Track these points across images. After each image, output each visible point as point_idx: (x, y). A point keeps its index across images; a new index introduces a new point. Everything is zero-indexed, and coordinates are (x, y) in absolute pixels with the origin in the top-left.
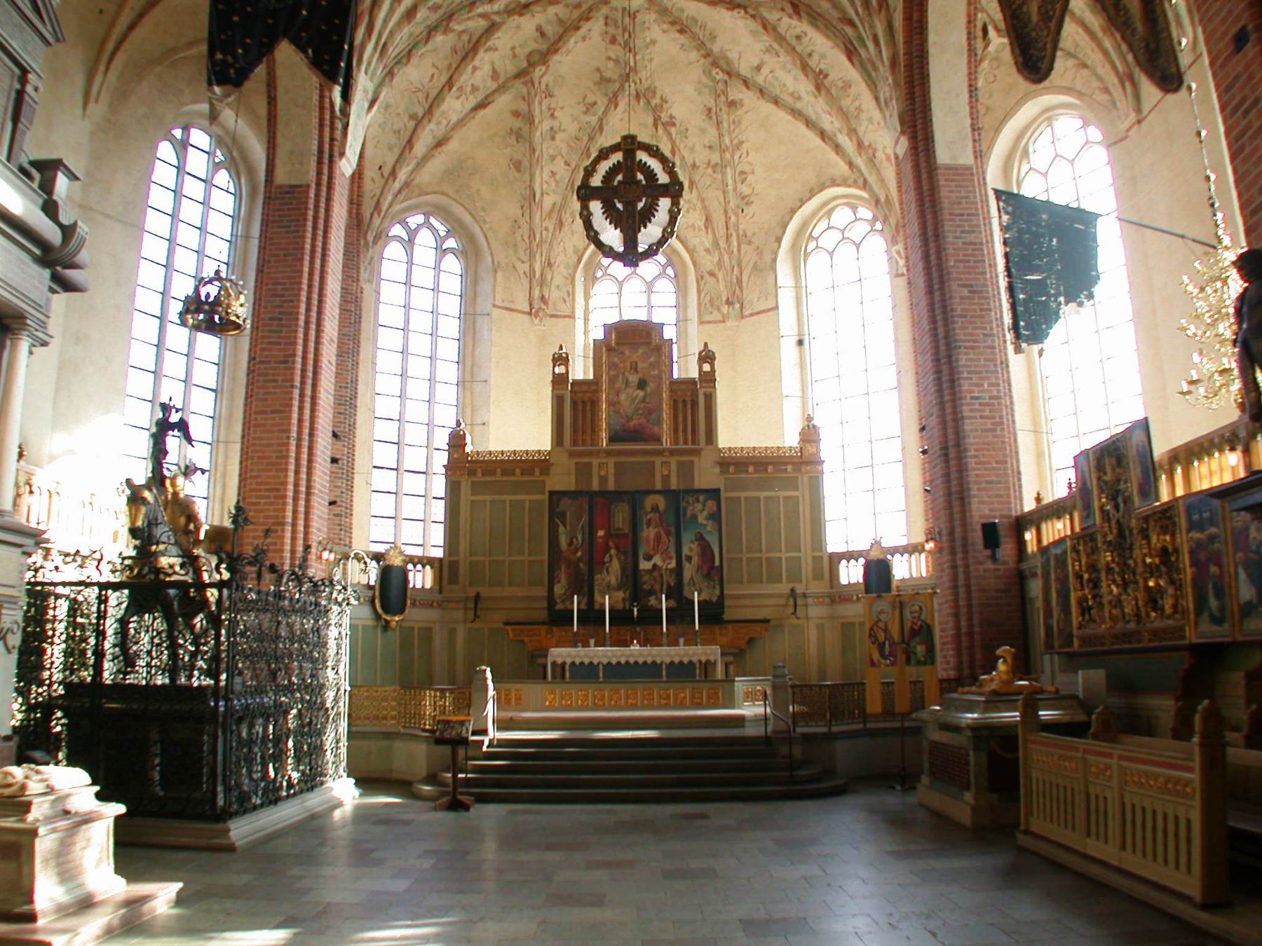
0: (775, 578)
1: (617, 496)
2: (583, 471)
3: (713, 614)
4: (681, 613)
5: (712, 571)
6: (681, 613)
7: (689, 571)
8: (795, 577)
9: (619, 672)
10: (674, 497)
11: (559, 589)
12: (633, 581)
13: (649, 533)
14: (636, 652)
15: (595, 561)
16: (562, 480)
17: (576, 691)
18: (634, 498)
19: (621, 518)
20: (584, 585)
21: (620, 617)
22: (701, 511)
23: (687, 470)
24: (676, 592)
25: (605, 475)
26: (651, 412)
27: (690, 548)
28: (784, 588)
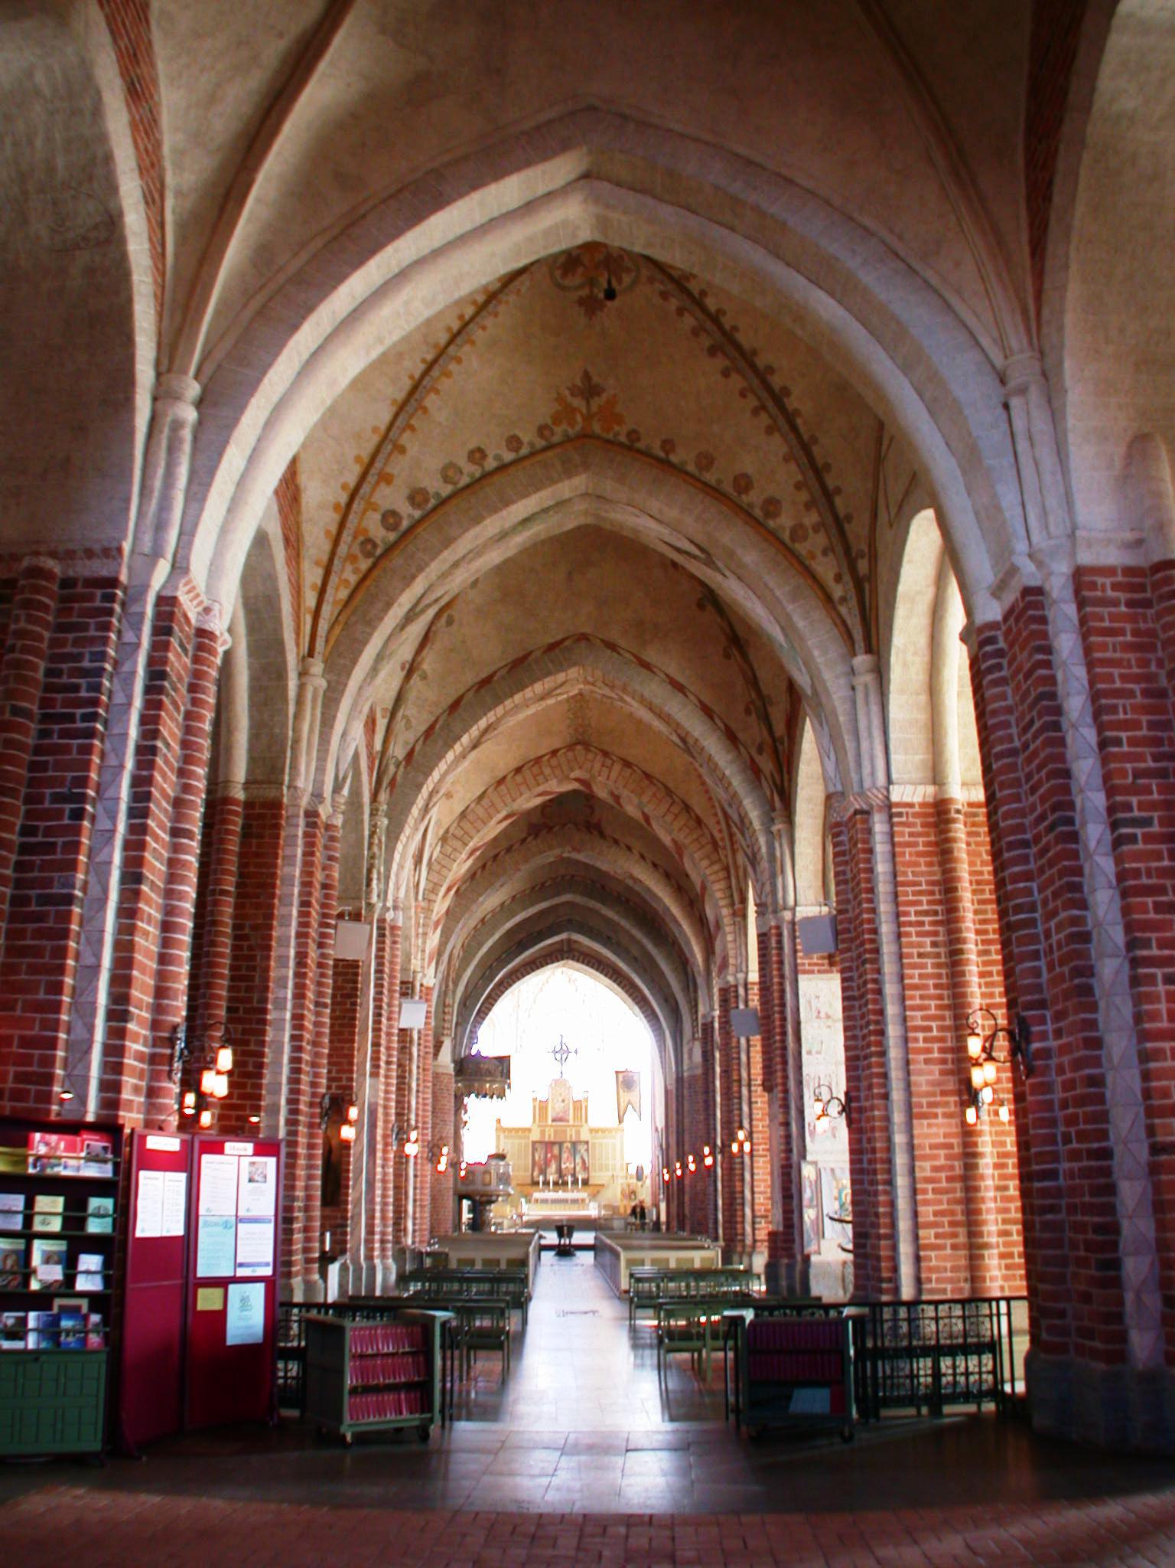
0: (607, 1170)
1: (553, 1143)
2: (543, 1132)
3: (586, 1182)
4: (575, 1182)
5: (585, 1168)
6: (575, 1182)
7: (578, 1168)
8: (614, 1169)
9: (555, 1201)
10: (574, 1144)
11: (536, 1173)
12: (560, 1172)
13: (565, 1156)
14: (561, 1195)
15: (547, 1163)
16: (535, 1136)
17: (544, 1206)
18: (561, 1144)
19: (556, 1150)
20: (543, 1172)
21: (556, 1184)
22: (582, 1148)
23: (578, 1133)
24: (574, 1175)
25: (550, 1136)
26: (566, 1112)
27: (578, 1160)
28: (610, 1174)
